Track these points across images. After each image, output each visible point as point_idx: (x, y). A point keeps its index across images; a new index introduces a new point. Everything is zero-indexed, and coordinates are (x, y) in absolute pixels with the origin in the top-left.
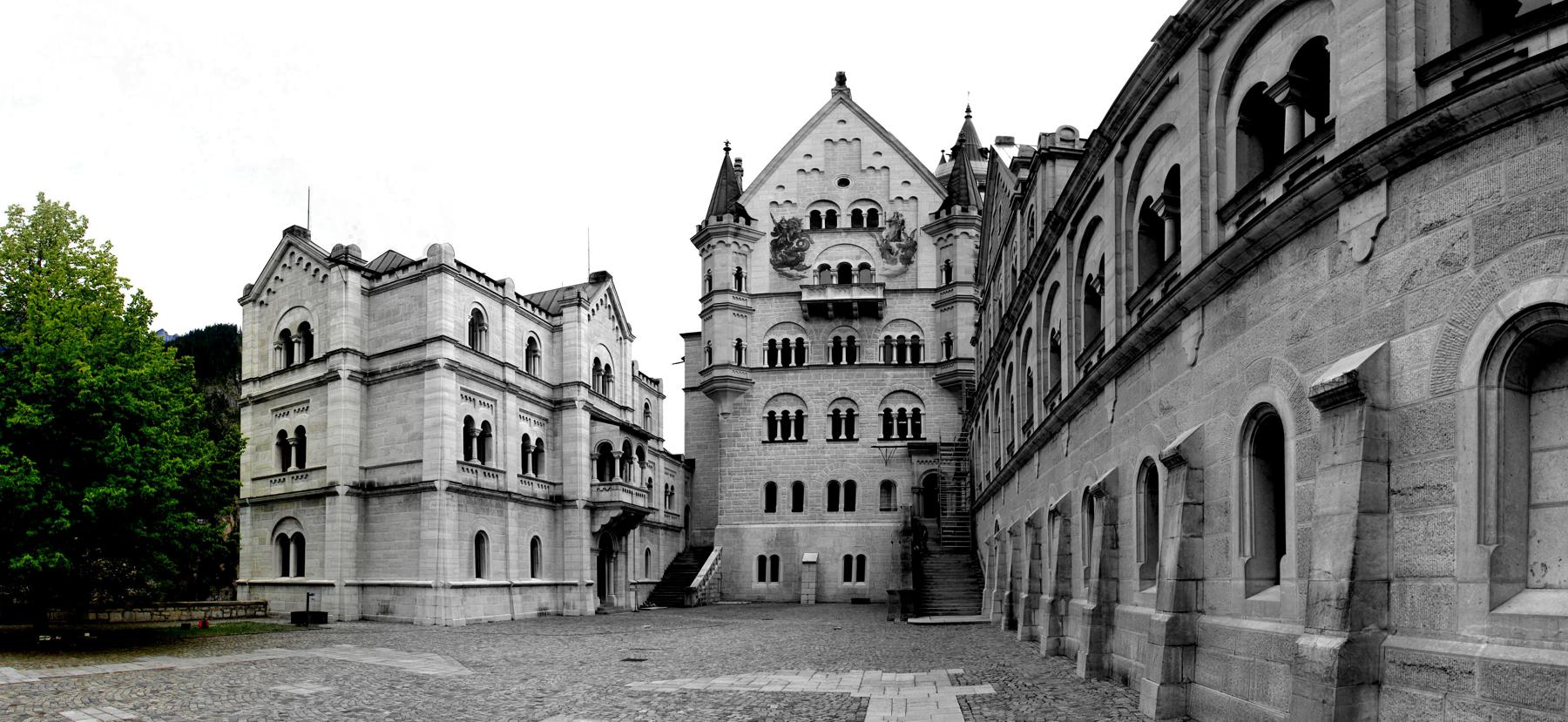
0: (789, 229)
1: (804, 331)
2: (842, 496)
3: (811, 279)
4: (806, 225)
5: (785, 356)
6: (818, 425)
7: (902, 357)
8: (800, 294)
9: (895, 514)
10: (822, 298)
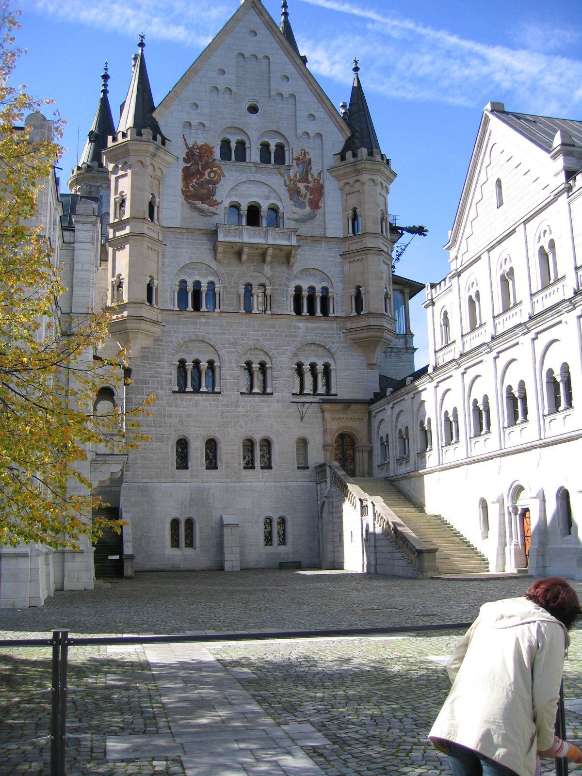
0: (201, 157)
1: (215, 273)
2: (257, 453)
3: (221, 215)
4: (217, 154)
5: (194, 298)
6: (231, 376)
7: (312, 311)
8: (215, 232)
9: (306, 472)
10: (237, 240)
